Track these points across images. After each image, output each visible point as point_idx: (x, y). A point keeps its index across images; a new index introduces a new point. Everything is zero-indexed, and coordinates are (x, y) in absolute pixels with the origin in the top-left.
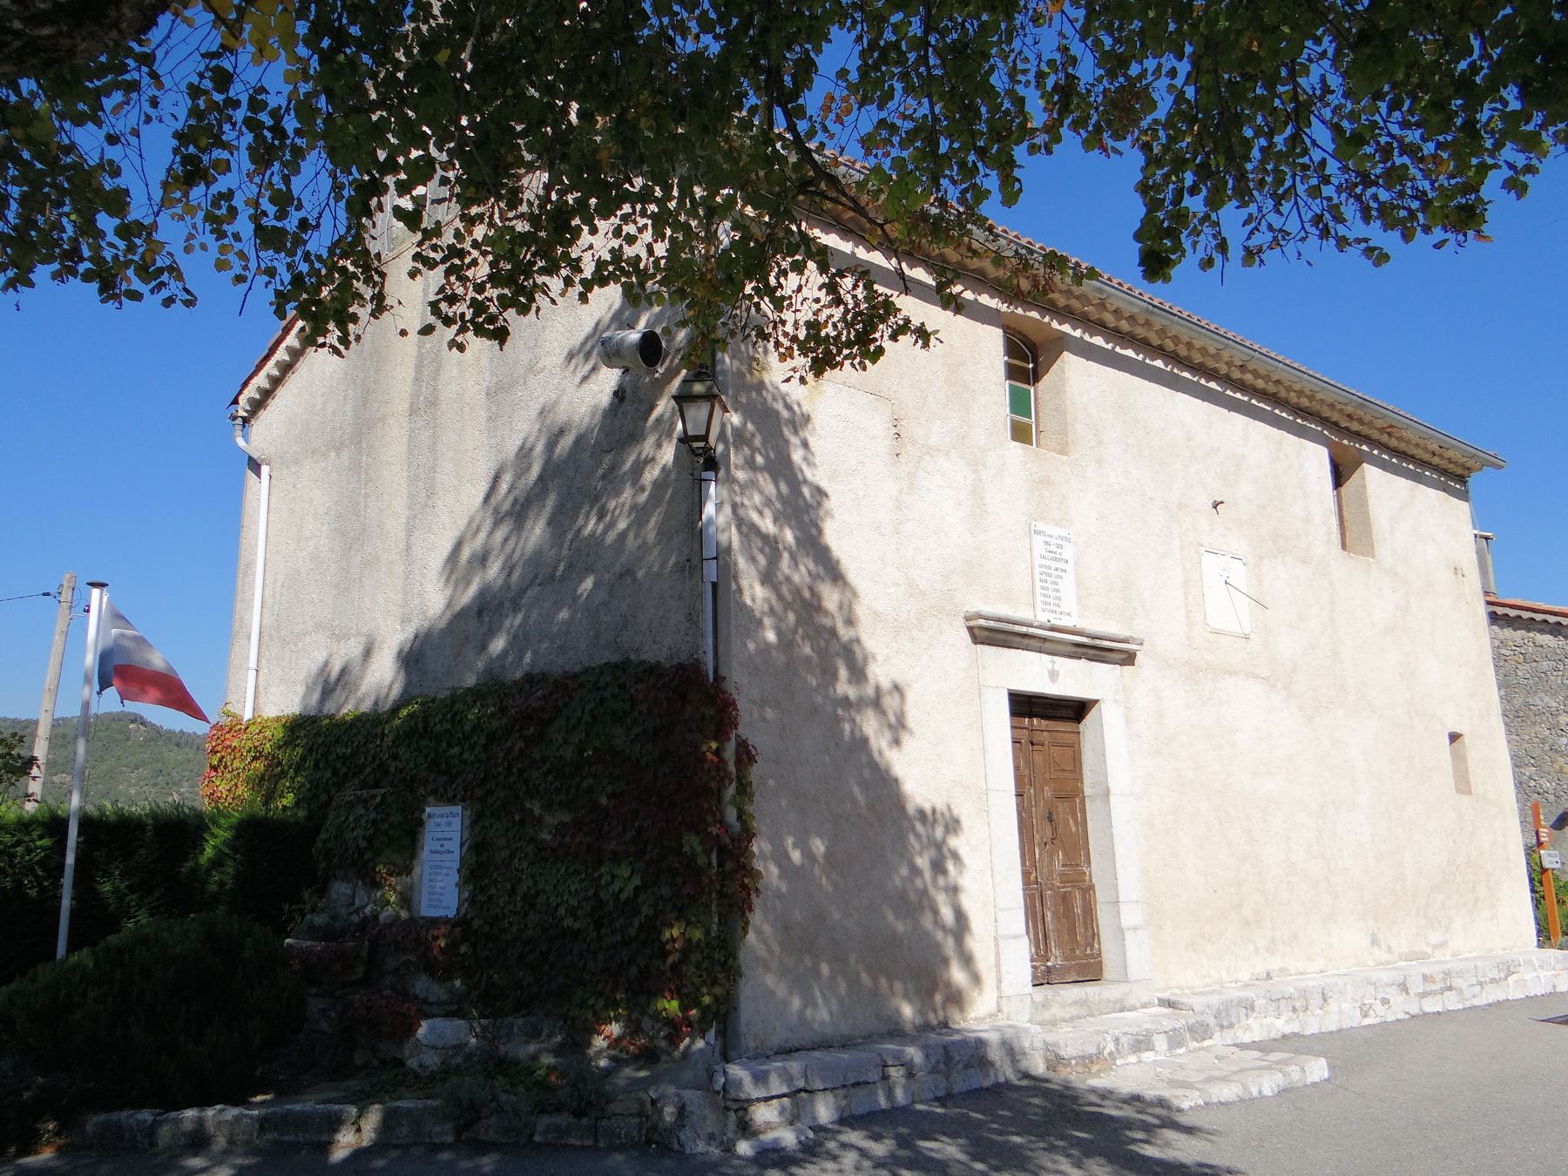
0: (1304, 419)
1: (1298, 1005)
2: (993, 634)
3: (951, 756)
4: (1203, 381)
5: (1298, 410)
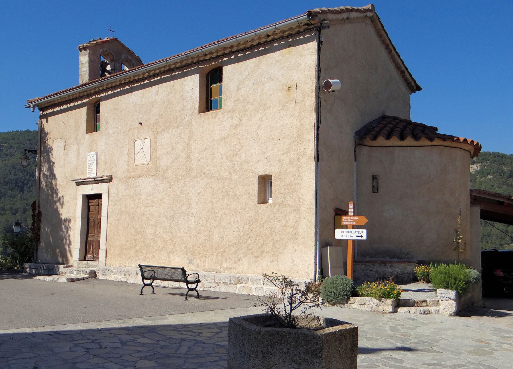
0: (188, 68)
1: (126, 274)
2: (79, 183)
3: (72, 210)
4: (142, 83)
5: (181, 68)
